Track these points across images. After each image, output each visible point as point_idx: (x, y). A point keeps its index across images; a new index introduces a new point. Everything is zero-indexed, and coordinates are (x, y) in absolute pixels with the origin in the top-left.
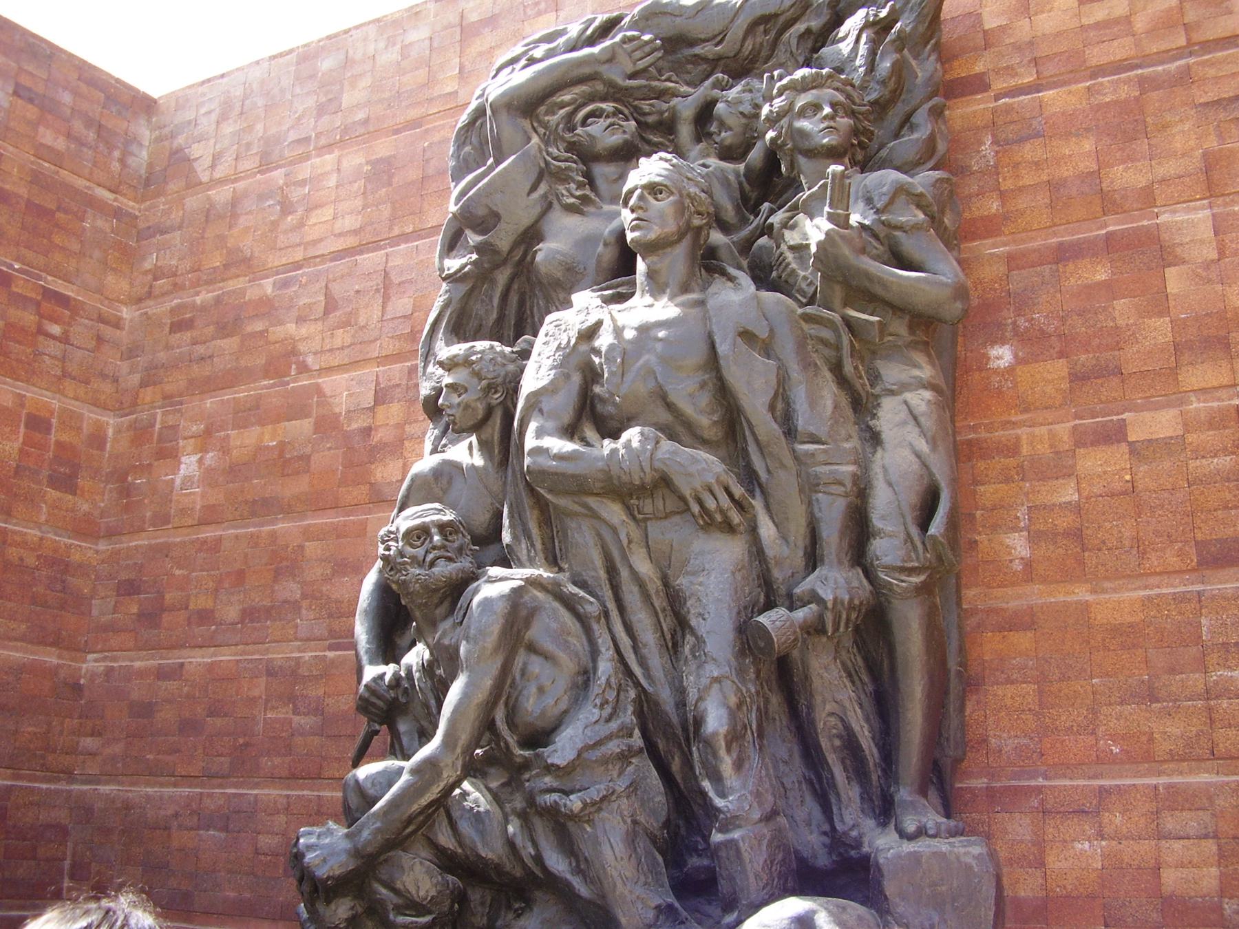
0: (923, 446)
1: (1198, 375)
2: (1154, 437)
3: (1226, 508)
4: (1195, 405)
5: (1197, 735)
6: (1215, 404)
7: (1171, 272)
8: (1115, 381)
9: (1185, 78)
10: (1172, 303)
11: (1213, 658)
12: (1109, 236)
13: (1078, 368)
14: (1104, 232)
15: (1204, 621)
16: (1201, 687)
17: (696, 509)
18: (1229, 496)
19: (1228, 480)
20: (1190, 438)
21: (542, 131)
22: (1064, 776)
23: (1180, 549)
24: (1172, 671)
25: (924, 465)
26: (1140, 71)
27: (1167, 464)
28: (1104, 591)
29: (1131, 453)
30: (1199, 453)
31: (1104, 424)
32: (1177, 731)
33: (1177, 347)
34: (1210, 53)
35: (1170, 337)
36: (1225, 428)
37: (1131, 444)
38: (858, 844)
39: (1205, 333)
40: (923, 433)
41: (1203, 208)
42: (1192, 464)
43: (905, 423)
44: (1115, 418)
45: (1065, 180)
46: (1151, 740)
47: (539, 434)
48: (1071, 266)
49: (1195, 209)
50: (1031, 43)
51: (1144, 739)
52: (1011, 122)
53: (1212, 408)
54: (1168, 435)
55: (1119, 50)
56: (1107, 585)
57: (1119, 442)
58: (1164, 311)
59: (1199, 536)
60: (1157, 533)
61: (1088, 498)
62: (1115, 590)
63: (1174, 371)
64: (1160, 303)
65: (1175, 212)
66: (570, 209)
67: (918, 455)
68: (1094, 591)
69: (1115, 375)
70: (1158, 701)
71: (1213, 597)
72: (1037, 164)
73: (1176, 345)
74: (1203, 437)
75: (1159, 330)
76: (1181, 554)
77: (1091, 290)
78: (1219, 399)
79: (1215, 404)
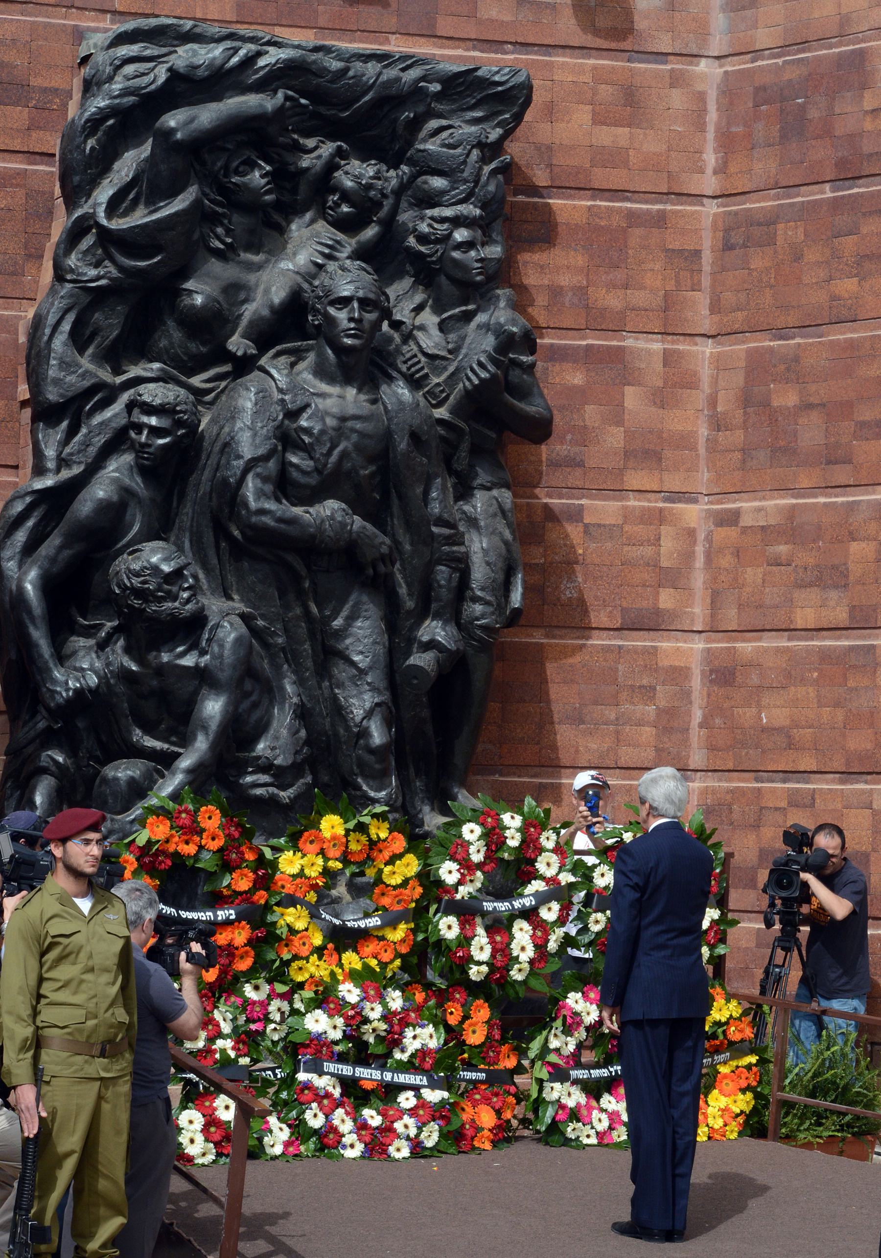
0: (508, 535)
1: (636, 479)
2: (602, 522)
3: (644, 585)
4: (633, 502)
5: (608, 750)
6: (646, 504)
7: (629, 390)
8: (578, 472)
9: (660, 220)
10: (626, 417)
11: (624, 695)
12: (589, 347)
13: (554, 455)
14: (584, 343)
15: (620, 667)
16: (613, 716)
17: (371, 572)
18: (646, 576)
19: (648, 565)
20: (626, 528)
21: (198, 167)
22: (514, 774)
23: (611, 612)
24: (596, 703)
25: (508, 551)
26: (629, 205)
27: (609, 545)
28: (554, 637)
29: (585, 532)
30: (632, 542)
31: (569, 505)
32: (595, 746)
33: (627, 454)
34: (682, 204)
35: (622, 445)
36: (651, 524)
37: (586, 526)
38: (422, 824)
39: (647, 446)
40: (509, 525)
41: (657, 341)
42: (626, 548)
43: (495, 515)
44: (576, 502)
45: (562, 288)
46: (577, 751)
47: (260, 494)
48: (558, 366)
49: (652, 340)
50: (549, 148)
51: (572, 750)
52: (526, 222)
53: (644, 507)
54: (613, 522)
55: (615, 178)
56: (557, 632)
57: (577, 521)
58: (620, 423)
59: (624, 604)
60: (596, 598)
61: (551, 563)
62: (561, 638)
63: (620, 472)
64: (617, 416)
65: (637, 339)
66: (220, 255)
67: (506, 543)
68: (547, 636)
69: (579, 466)
70: (583, 723)
71: (628, 651)
72: (542, 267)
73: (626, 452)
74: (635, 528)
75: (614, 438)
76: (610, 615)
77: (573, 390)
78: (649, 501)
79: (646, 504)
